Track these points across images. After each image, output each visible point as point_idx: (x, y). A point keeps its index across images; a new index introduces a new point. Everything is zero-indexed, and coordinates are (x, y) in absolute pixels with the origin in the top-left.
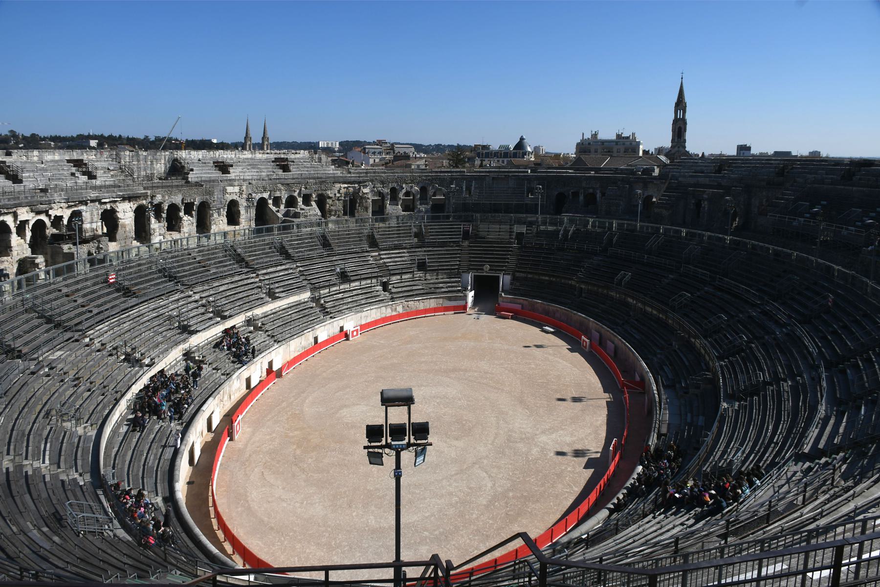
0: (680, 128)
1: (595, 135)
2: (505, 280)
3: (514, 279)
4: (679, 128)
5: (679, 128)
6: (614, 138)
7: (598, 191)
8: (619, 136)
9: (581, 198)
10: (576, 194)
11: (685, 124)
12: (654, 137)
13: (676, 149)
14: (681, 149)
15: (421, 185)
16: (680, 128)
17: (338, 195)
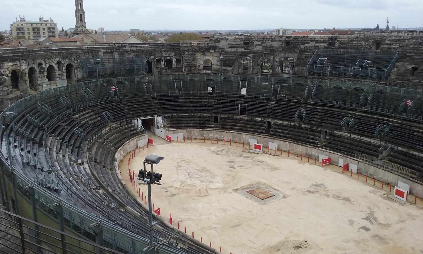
0: (81, 15)
1: (23, 19)
2: (159, 120)
3: (166, 119)
4: (80, 16)
5: (80, 16)
6: (37, 20)
7: (174, 58)
8: (40, 19)
9: (163, 63)
10: (159, 61)
11: (84, 12)
12: (66, 21)
13: (81, 28)
14: (83, 28)
15: (57, 59)
16: (81, 15)
17: (8, 72)
